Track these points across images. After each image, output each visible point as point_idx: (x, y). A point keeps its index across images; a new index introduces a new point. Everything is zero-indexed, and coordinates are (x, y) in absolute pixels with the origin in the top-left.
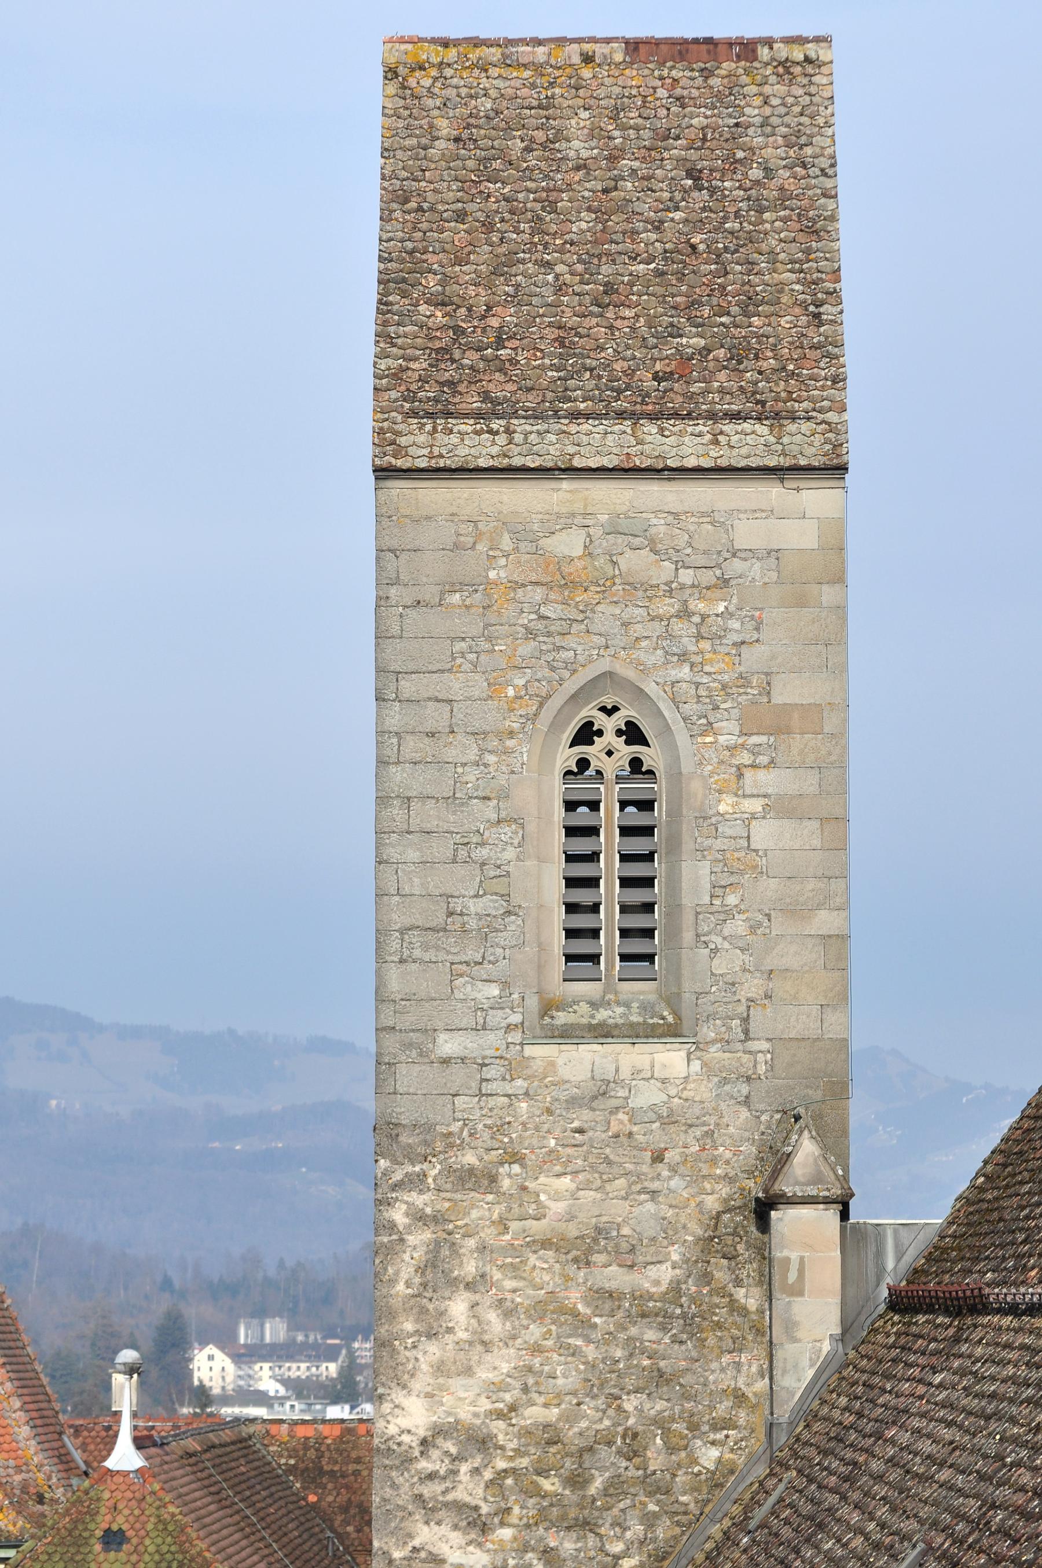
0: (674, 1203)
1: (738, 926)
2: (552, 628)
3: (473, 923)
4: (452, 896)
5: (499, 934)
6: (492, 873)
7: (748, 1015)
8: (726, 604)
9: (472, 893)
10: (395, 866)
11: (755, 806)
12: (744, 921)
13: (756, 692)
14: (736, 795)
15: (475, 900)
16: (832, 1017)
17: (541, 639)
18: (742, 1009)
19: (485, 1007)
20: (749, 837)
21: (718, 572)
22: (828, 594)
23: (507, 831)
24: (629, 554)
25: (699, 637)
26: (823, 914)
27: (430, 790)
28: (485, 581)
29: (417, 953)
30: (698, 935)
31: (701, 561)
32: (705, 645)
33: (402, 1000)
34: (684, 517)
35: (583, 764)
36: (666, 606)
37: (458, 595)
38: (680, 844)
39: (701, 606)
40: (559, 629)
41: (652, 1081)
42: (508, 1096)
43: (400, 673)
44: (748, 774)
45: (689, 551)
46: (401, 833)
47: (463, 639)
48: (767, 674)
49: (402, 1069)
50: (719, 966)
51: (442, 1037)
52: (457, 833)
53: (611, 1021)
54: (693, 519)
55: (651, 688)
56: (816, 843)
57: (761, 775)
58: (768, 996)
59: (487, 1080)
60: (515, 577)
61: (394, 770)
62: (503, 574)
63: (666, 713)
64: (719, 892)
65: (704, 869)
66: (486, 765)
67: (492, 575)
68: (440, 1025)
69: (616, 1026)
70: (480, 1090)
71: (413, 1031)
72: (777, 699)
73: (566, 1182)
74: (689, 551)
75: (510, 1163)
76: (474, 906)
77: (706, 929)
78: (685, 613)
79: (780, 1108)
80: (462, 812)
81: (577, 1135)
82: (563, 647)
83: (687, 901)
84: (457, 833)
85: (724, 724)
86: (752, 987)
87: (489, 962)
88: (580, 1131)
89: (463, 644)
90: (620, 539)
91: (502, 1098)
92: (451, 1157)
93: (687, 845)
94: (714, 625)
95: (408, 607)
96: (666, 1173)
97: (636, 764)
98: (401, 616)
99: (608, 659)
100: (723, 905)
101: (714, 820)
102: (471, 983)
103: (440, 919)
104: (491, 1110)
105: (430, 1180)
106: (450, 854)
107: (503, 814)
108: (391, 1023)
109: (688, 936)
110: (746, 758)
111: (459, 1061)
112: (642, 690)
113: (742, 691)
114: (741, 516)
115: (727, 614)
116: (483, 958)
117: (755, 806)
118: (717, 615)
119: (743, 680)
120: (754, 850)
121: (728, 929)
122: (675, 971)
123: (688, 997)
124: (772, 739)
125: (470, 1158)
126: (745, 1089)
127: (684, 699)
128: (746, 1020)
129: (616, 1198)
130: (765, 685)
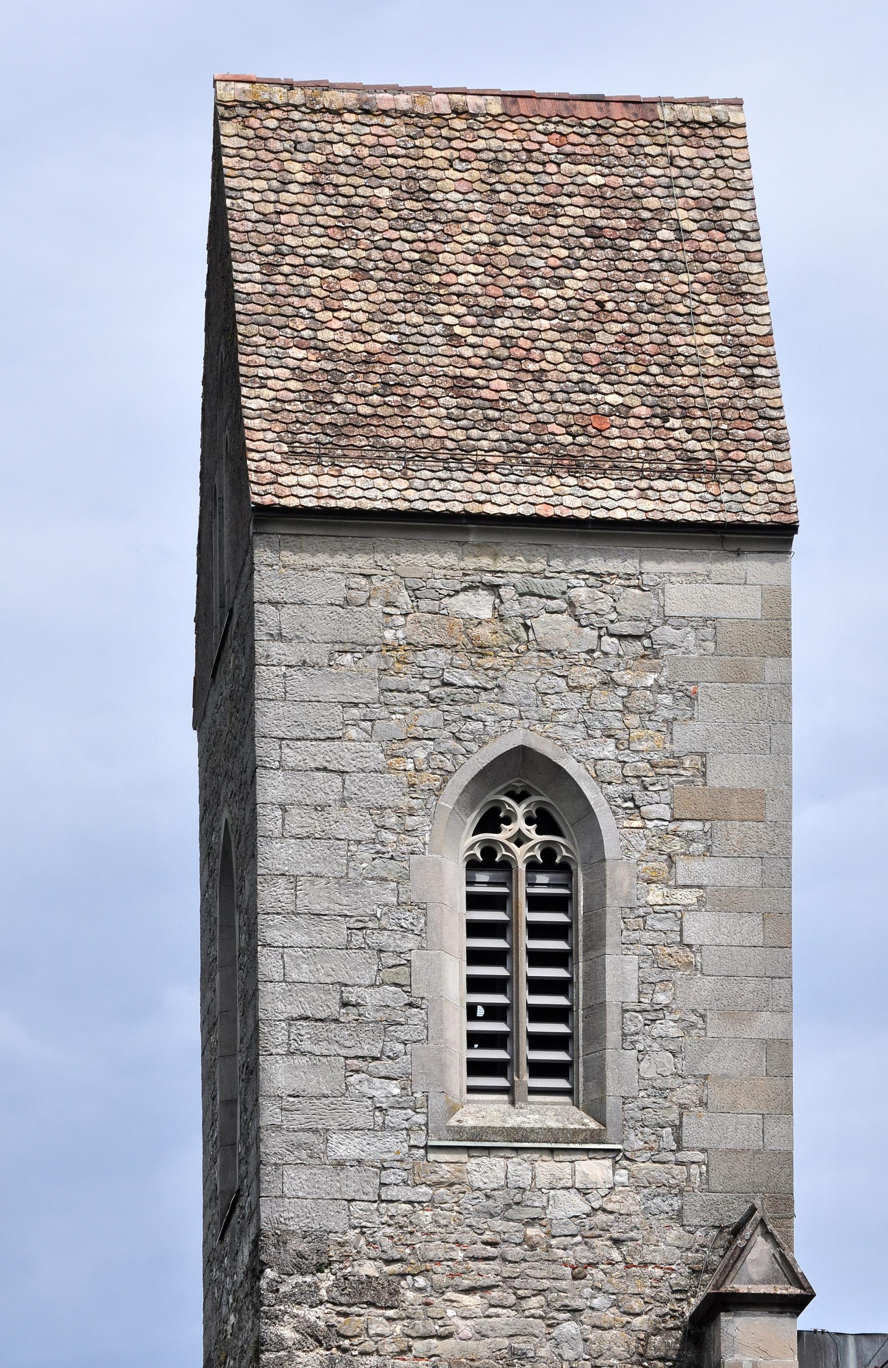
0: (598, 1323)
1: (668, 1027)
2: (458, 697)
3: (370, 1015)
4: (346, 985)
5: (400, 1028)
6: (391, 962)
7: (681, 1122)
8: (656, 676)
9: (368, 983)
10: (281, 950)
11: (688, 897)
12: (675, 1021)
13: (689, 774)
14: (668, 886)
15: (371, 990)
16: (773, 1129)
17: (446, 708)
18: (674, 1116)
19: (384, 1106)
20: (681, 930)
21: (646, 642)
22: (771, 669)
23: (407, 918)
24: (545, 617)
25: (626, 709)
26: (765, 1016)
27: (316, 869)
28: (380, 641)
29: (307, 1046)
30: (624, 1035)
31: (625, 628)
32: (633, 720)
33: (290, 1096)
34: (607, 579)
35: (489, 850)
36: (585, 676)
37: (349, 656)
38: (603, 938)
39: (627, 677)
40: (466, 698)
41: (573, 1191)
42: (411, 1202)
43: (283, 739)
44: (681, 862)
45: (613, 616)
46: (286, 914)
47: (356, 705)
48: (703, 755)
49: (290, 1172)
50: (648, 1069)
51: (335, 1138)
52: (351, 917)
53: (526, 1126)
54: (618, 581)
55: (570, 765)
56: (758, 940)
57: (696, 865)
58: (703, 1104)
59: (385, 1185)
60: (415, 639)
61: (279, 845)
62: (400, 634)
63: (588, 794)
64: (648, 989)
65: (631, 963)
66: (382, 843)
67: (389, 635)
68: (334, 1126)
69: (533, 1130)
70: (379, 1196)
71: (303, 1130)
72: (713, 782)
73: (472, 1301)
74: (613, 616)
75: (414, 1275)
76: (371, 997)
77: (633, 1029)
78: (609, 683)
79: (717, 1224)
80: (357, 894)
81: (488, 1247)
82: (470, 717)
83: (612, 997)
84: (351, 917)
85: (653, 807)
86: (686, 1093)
87: (389, 1057)
88: (494, 1244)
89: (355, 711)
90: (534, 601)
91: (404, 1206)
92: (346, 1267)
93: (612, 939)
94: (641, 699)
95: (290, 666)
96: (587, 1291)
97: (548, 852)
98: (285, 675)
99: (522, 731)
100: (652, 1003)
101: (641, 912)
102: (367, 1080)
103: (334, 1009)
104: (392, 1217)
105: (323, 1292)
106: (342, 939)
107: (404, 898)
108: (277, 1122)
109: (613, 1035)
110: (677, 845)
111: (355, 1163)
112: (560, 768)
113: (673, 771)
114: (673, 579)
115: (659, 688)
116: (382, 1052)
117: (688, 897)
118: (646, 688)
119: (675, 762)
120: (689, 946)
121: (657, 1029)
122: (597, 1076)
123: (612, 1103)
124: (708, 825)
125: (368, 1269)
126: (677, 1203)
127: (608, 779)
128: (677, 1129)
129: (533, 1316)
130: (699, 766)
